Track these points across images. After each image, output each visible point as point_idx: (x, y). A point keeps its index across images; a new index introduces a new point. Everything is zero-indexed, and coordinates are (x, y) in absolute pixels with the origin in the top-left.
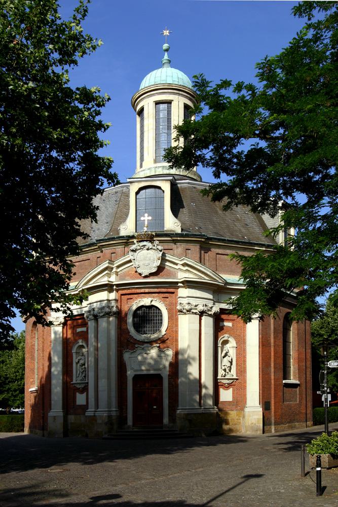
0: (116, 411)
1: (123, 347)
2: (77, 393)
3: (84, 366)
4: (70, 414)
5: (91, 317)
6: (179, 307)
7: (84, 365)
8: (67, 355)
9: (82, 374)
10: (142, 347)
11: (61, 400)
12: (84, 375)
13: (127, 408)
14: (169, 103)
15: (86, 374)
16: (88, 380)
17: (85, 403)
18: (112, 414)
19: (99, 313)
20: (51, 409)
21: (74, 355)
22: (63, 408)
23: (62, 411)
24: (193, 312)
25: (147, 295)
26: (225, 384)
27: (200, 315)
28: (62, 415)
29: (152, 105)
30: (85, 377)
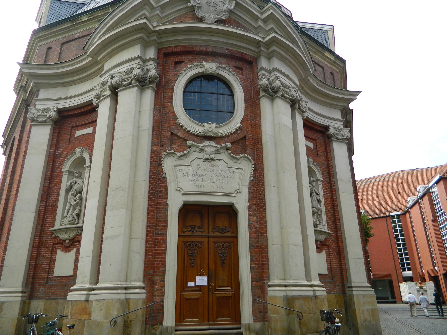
2: (59, 252)
4: (38, 298)
7: (81, 192)
8: (51, 176)
9: (74, 210)
11: (24, 263)
12: (77, 212)
13: (163, 281)
15: (80, 211)
17: (70, 273)
18: (132, 296)
21: (65, 177)
28: (19, 299)
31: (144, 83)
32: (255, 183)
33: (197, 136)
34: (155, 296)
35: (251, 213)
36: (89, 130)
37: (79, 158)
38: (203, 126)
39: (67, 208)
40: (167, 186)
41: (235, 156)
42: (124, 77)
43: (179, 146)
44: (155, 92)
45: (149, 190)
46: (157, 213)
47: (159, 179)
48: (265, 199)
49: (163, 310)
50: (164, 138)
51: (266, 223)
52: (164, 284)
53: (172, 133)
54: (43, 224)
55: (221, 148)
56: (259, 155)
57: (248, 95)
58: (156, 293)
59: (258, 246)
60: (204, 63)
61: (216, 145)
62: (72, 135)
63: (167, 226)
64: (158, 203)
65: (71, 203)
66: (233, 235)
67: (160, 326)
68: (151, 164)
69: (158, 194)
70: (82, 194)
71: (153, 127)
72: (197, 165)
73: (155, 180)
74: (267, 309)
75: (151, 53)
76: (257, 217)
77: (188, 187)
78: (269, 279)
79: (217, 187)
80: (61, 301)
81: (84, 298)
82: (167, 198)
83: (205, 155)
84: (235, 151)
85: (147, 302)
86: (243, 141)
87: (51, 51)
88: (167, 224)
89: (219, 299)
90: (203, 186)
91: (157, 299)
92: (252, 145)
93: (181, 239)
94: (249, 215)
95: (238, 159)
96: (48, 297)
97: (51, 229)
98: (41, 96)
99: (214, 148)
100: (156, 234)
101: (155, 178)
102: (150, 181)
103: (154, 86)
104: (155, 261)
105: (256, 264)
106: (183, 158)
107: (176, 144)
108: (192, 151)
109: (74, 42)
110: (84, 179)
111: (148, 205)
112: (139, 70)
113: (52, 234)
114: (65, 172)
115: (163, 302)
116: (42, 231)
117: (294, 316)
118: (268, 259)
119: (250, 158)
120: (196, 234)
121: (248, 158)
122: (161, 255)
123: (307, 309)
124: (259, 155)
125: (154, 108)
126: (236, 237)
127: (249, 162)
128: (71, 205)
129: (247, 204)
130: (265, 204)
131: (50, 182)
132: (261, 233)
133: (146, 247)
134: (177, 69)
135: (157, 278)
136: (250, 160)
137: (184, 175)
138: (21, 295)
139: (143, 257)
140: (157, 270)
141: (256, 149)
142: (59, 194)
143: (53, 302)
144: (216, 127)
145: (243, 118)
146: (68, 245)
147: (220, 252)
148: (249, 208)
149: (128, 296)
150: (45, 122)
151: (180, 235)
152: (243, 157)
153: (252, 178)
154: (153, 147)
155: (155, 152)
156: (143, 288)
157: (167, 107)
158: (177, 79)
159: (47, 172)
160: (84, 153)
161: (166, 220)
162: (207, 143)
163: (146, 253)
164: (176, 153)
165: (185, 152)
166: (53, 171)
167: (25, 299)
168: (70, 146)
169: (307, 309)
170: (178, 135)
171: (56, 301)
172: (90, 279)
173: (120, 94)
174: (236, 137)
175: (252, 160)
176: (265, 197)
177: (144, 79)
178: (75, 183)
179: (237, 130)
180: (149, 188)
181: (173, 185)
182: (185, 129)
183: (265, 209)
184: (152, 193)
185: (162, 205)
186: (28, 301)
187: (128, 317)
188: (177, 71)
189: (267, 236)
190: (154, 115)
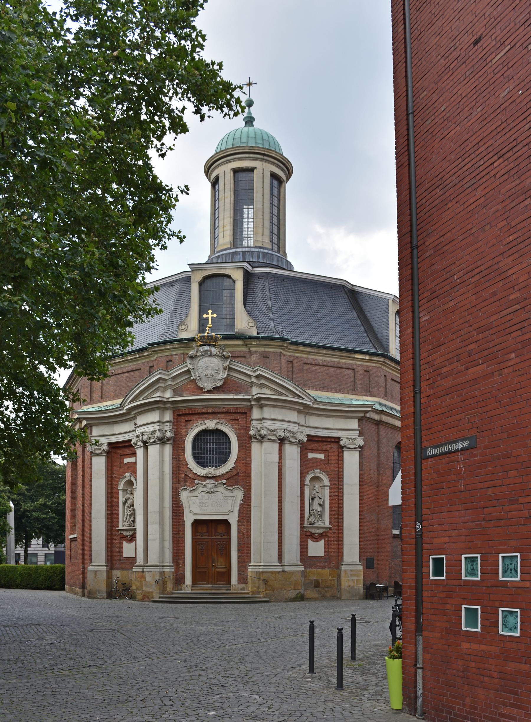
2: (124, 543)
3: (132, 508)
4: (116, 569)
5: (140, 444)
7: (133, 505)
9: (130, 517)
11: (104, 549)
12: (132, 519)
13: (184, 563)
14: (252, 170)
18: (166, 570)
20: (91, 562)
21: (121, 494)
24: (269, 439)
25: (211, 416)
27: (279, 443)
28: (105, 569)
39: (125, 516)
60: (205, 421)
62: (121, 462)
75: (168, 416)
80: (130, 571)
91: (181, 572)
96: (122, 569)
103: (171, 442)
116: (111, 530)
134: (187, 426)
135: (181, 562)
137: (194, 503)
139: (172, 550)
143: (126, 572)
149: (164, 570)
161: (184, 530)
167: (108, 569)
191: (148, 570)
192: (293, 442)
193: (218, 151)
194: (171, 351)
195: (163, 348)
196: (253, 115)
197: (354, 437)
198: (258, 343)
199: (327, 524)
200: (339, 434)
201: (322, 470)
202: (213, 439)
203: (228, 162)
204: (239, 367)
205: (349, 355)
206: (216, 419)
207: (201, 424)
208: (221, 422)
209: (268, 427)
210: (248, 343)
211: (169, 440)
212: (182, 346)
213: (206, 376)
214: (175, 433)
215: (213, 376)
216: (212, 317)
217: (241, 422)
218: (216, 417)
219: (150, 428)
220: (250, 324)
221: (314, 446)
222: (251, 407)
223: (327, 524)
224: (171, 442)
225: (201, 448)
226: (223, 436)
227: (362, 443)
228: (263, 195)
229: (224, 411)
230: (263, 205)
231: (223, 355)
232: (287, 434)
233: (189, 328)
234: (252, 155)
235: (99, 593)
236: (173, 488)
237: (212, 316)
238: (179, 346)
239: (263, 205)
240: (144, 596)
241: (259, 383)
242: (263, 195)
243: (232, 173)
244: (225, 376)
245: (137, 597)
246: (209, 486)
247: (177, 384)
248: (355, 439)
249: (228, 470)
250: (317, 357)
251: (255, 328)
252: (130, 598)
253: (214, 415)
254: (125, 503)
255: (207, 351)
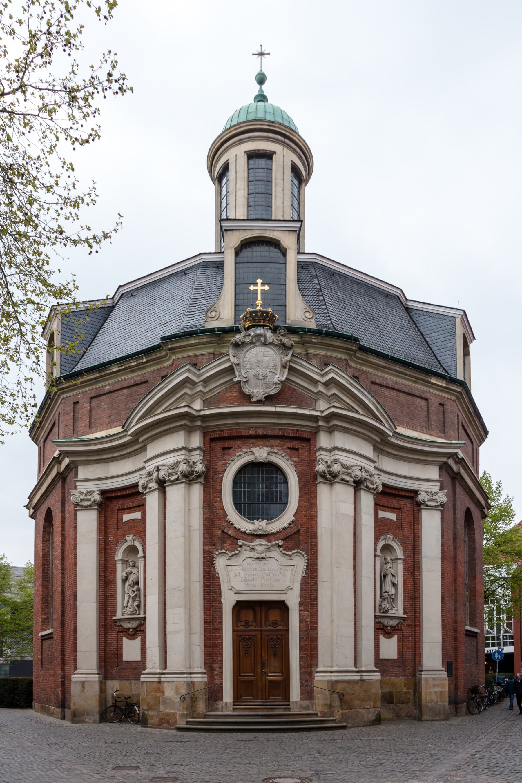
0: (201, 673)
1: (214, 545)
2: (125, 640)
3: (136, 586)
4: (113, 679)
6: (321, 467)
7: (137, 583)
8: (105, 565)
9: (134, 600)
10: (251, 544)
12: (136, 603)
13: (221, 668)
14: (269, 156)
15: (140, 602)
16: (145, 613)
17: (139, 658)
18: (196, 680)
19: (169, 476)
20: (76, 668)
21: (119, 566)
22: (100, 667)
23: (96, 672)
25: (260, 442)
26: (387, 627)
28: (97, 679)
29: (243, 160)
30: (138, 606)
31: (191, 478)
32: (308, 578)
33: (248, 534)
34: (215, 679)
35: (302, 608)
36: (137, 515)
37: (130, 546)
38: (254, 524)
40: (220, 585)
41: (287, 553)
42: (170, 471)
43: (230, 545)
44: (204, 486)
45: (204, 590)
46: (213, 611)
47: (213, 578)
48: (317, 595)
49: (222, 690)
50: (215, 536)
51: (317, 617)
52: (222, 670)
53: (223, 531)
54: (105, 613)
55: (272, 546)
56: (313, 549)
57: (303, 481)
58: (216, 677)
59: (308, 638)
61: (266, 543)
63: (222, 622)
64: (213, 601)
65: (130, 594)
66: (285, 628)
67: (221, 702)
68: (204, 564)
69: (213, 592)
70: (138, 585)
71: (204, 525)
72: (249, 564)
73: (209, 580)
74: (313, 690)
75: (196, 441)
76: (308, 611)
77: (240, 586)
78: (317, 666)
79: (268, 586)
81: (156, 680)
82: (221, 597)
83: (256, 554)
84: (288, 547)
85: (209, 684)
86: (296, 536)
87: (78, 406)
88: (222, 620)
89: (271, 682)
90: (255, 586)
91: (217, 682)
92: (306, 538)
93: (236, 633)
94: (300, 610)
95: (290, 556)
97: (113, 618)
98: (80, 476)
99: (265, 547)
100: (213, 629)
101: (209, 578)
102: (204, 581)
103: (202, 480)
104: (213, 652)
105: (305, 654)
106: (234, 557)
107: (228, 542)
108: (243, 550)
109: (104, 397)
110: (139, 569)
111: (204, 604)
112: (185, 465)
113: (116, 622)
114: (118, 560)
115: (222, 684)
116: (105, 620)
117: (336, 696)
118: (317, 649)
119: (303, 553)
120: (250, 628)
121: (301, 554)
122: (219, 647)
123: (349, 691)
124: (313, 549)
125: (204, 505)
126: (288, 630)
127: (302, 557)
128: (130, 596)
129: (299, 600)
130: (317, 599)
131: (105, 571)
132: (311, 627)
133: (205, 640)
135: (216, 666)
136: (303, 555)
137: (236, 575)
138: (98, 676)
140: (216, 659)
141: (311, 543)
142: (116, 583)
143: (127, 682)
144: (267, 524)
145: (297, 509)
146: (132, 633)
147: (272, 644)
148: (301, 604)
149: (193, 679)
150: (90, 506)
151: (235, 629)
152: (296, 553)
153: (304, 574)
154: (205, 547)
155: (207, 552)
156: (205, 673)
157: (216, 502)
158: (226, 469)
159: (100, 561)
160: (135, 542)
161: (221, 617)
162: (257, 541)
163: (205, 645)
164: (227, 552)
165: (237, 552)
166: (106, 560)
167: (101, 679)
168: (119, 532)
169: (349, 691)
170: (229, 533)
171: (129, 681)
172: (160, 666)
173: (168, 489)
174: (288, 532)
175: (305, 555)
176: (317, 592)
177: (191, 473)
178: (130, 574)
179: (290, 524)
180: (204, 588)
181: (226, 584)
182: (235, 527)
183: (317, 604)
184: (207, 592)
185: (216, 603)
186: (104, 681)
187: (194, 695)
188: (225, 460)
189: (317, 629)
190: (204, 512)
191: (168, 680)
192: (370, 489)
193: (228, 127)
194: (196, 349)
195: (185, 343)
196: (265, 93)
197: (435, 491)
198: (319, 341)
199: (401, 613)
200: (416, 486)
201: (396, 536)
202: (263, 477)
203: (241, 142)
204: (303, 366)
205: (424, 378)
206: (267, 446)
207: (246, 452)
208: (276, 451)
209: (341, 461)
210: (307, 339)
211: (198, 476)
212: (214, 339)
213: (256, 376)
214: (207, 467)
215: (266, 376)
216: (261, 290)
217: (303, 453)
218: (267, 443)
219: (170, 459)
220: (307, 315)
221: (386, 501)
222: (316, 432)
223: (401, 613)
224: (202, 480)
225: (245, 491)
226: (276, 473)
227: (445, 500)
228: (284, 190)
229: (280, 433)
230: (283, 203)
231: (283, 344)
232: (364, 474)
233: (222, 316)
234: (271, 135)
235: (88, 714)
236: (204, 552)
237: (263, 288)
238: (209, 340)
239: (283, 203)
240: (161, 719)
241: (329, 394)
242: (284, 190)
243: (246, 157)
244: (284, 378)
245: (150, 721)
246: (260, 549)
247: (210, 391)
248: (436, 493)
249: (285, 525)
250: (387, 376)
251: (313, 320)
252: (137, 722)
253: (265, 441)
254: (125, 580)
255: (260, 335)
